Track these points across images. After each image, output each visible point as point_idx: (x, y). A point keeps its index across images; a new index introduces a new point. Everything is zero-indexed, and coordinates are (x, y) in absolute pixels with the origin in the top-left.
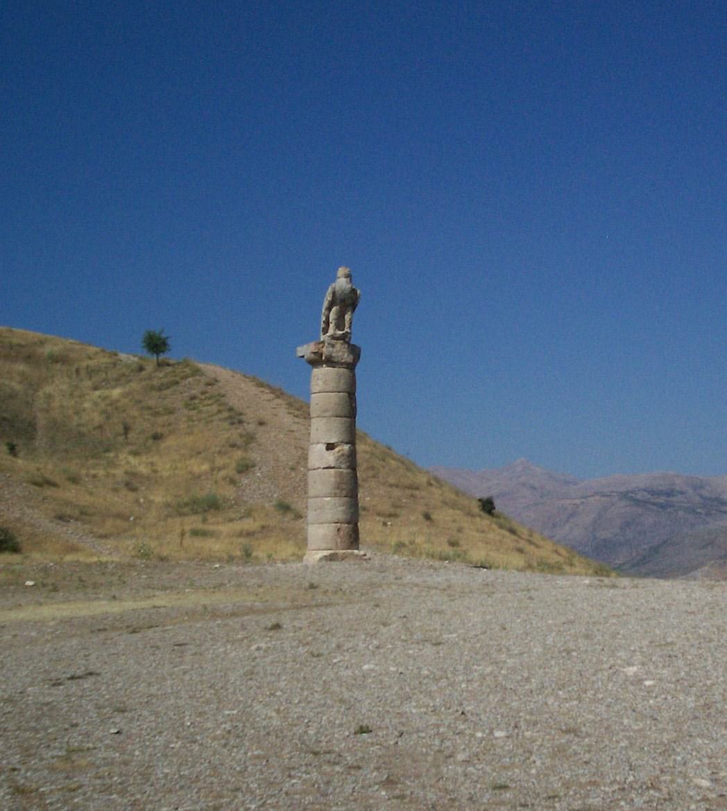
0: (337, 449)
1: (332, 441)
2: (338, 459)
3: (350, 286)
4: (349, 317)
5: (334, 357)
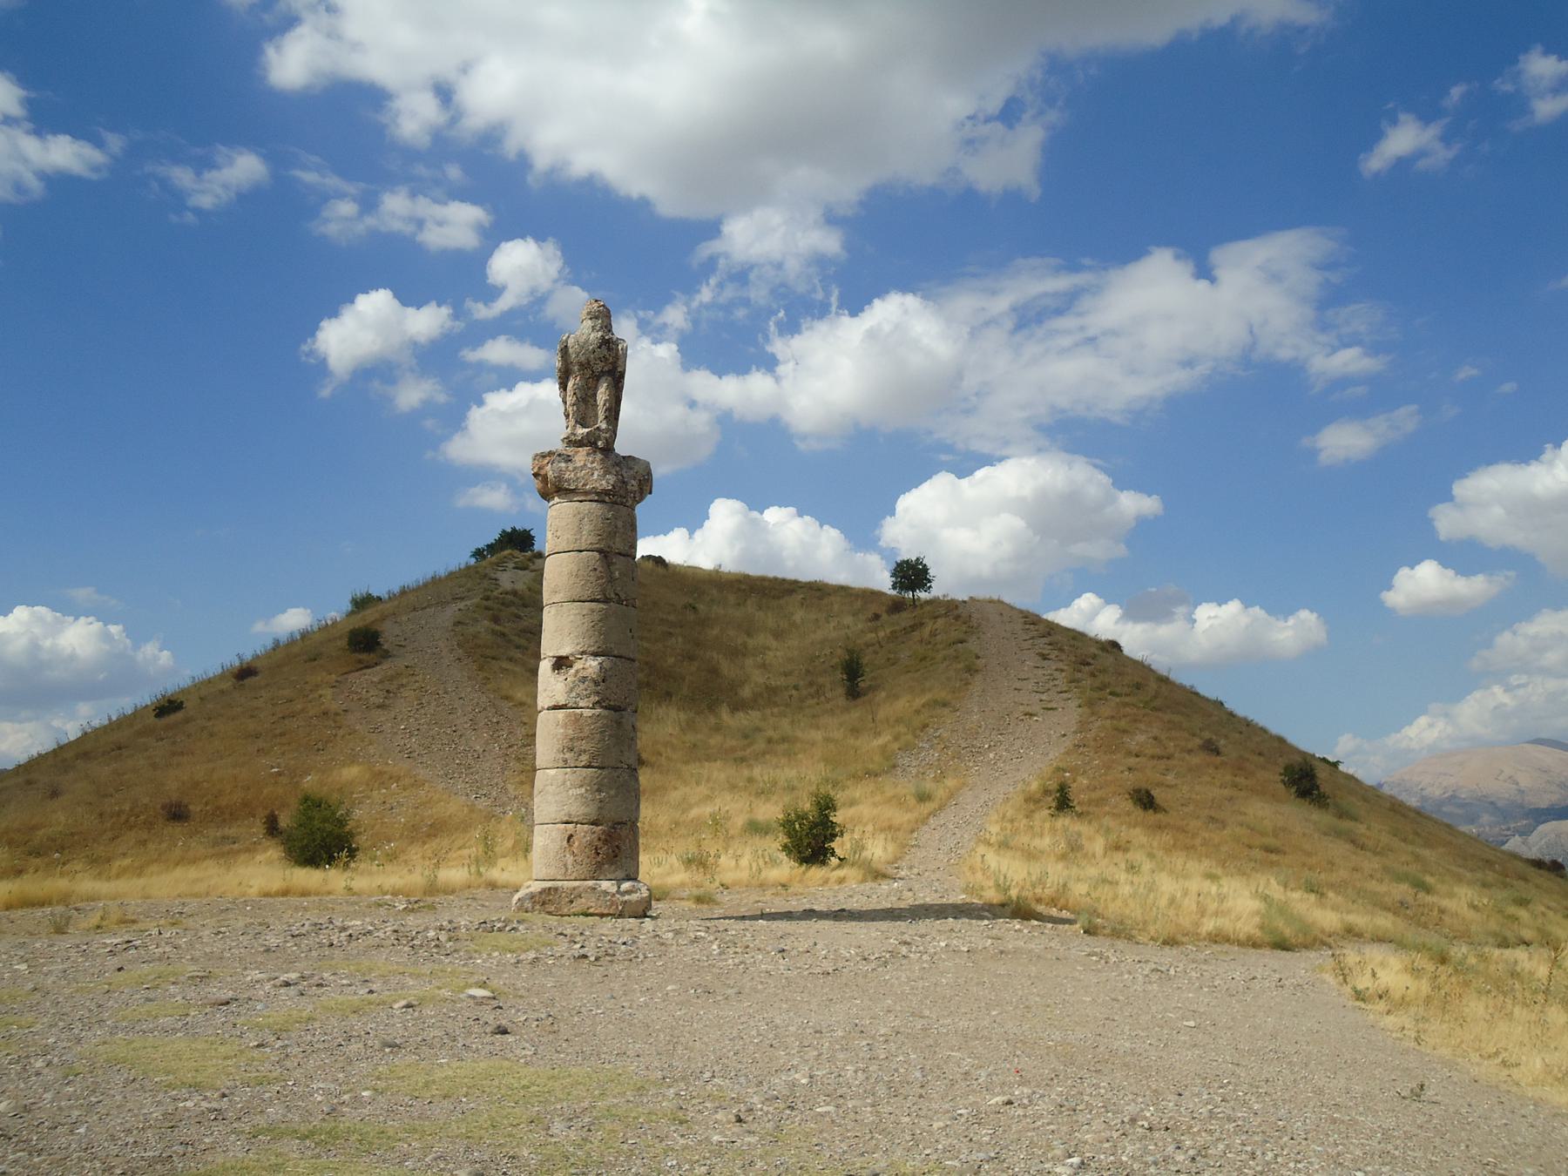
0: (572, 671)
1: (563, 653)
2: (571, 690)
3: (600, 334)
5: (568, 481)
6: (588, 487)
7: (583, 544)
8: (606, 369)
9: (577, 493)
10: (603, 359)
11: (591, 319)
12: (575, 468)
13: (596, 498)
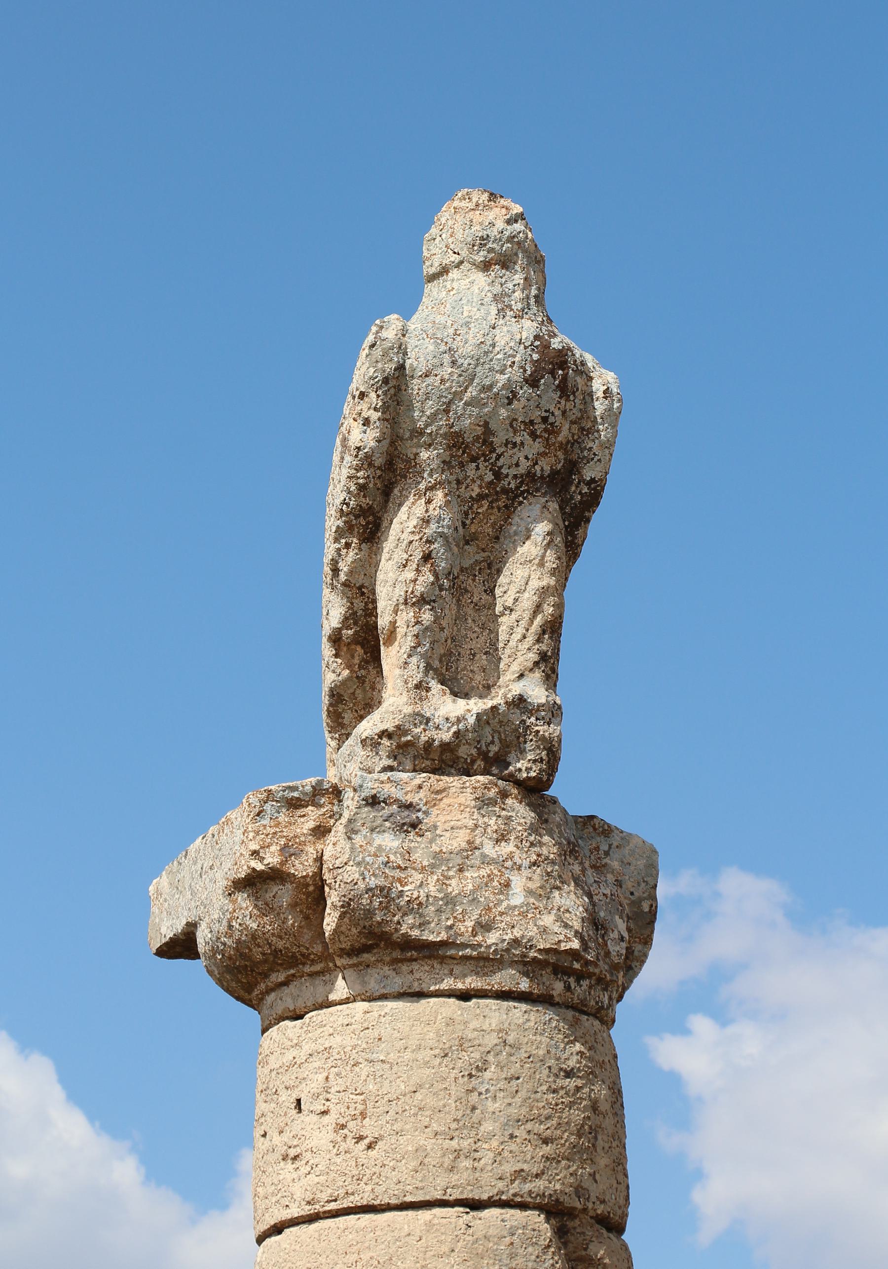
3: (528, 328)
4: (540, 580)
5: (415, 907)
6: (492, 938)
7: (486, 1178)
8: (545, 466)
9: (443, 959)
10: (539, 428)
11: (486, 266)
12: (439, 858)
13: (524, 985)
